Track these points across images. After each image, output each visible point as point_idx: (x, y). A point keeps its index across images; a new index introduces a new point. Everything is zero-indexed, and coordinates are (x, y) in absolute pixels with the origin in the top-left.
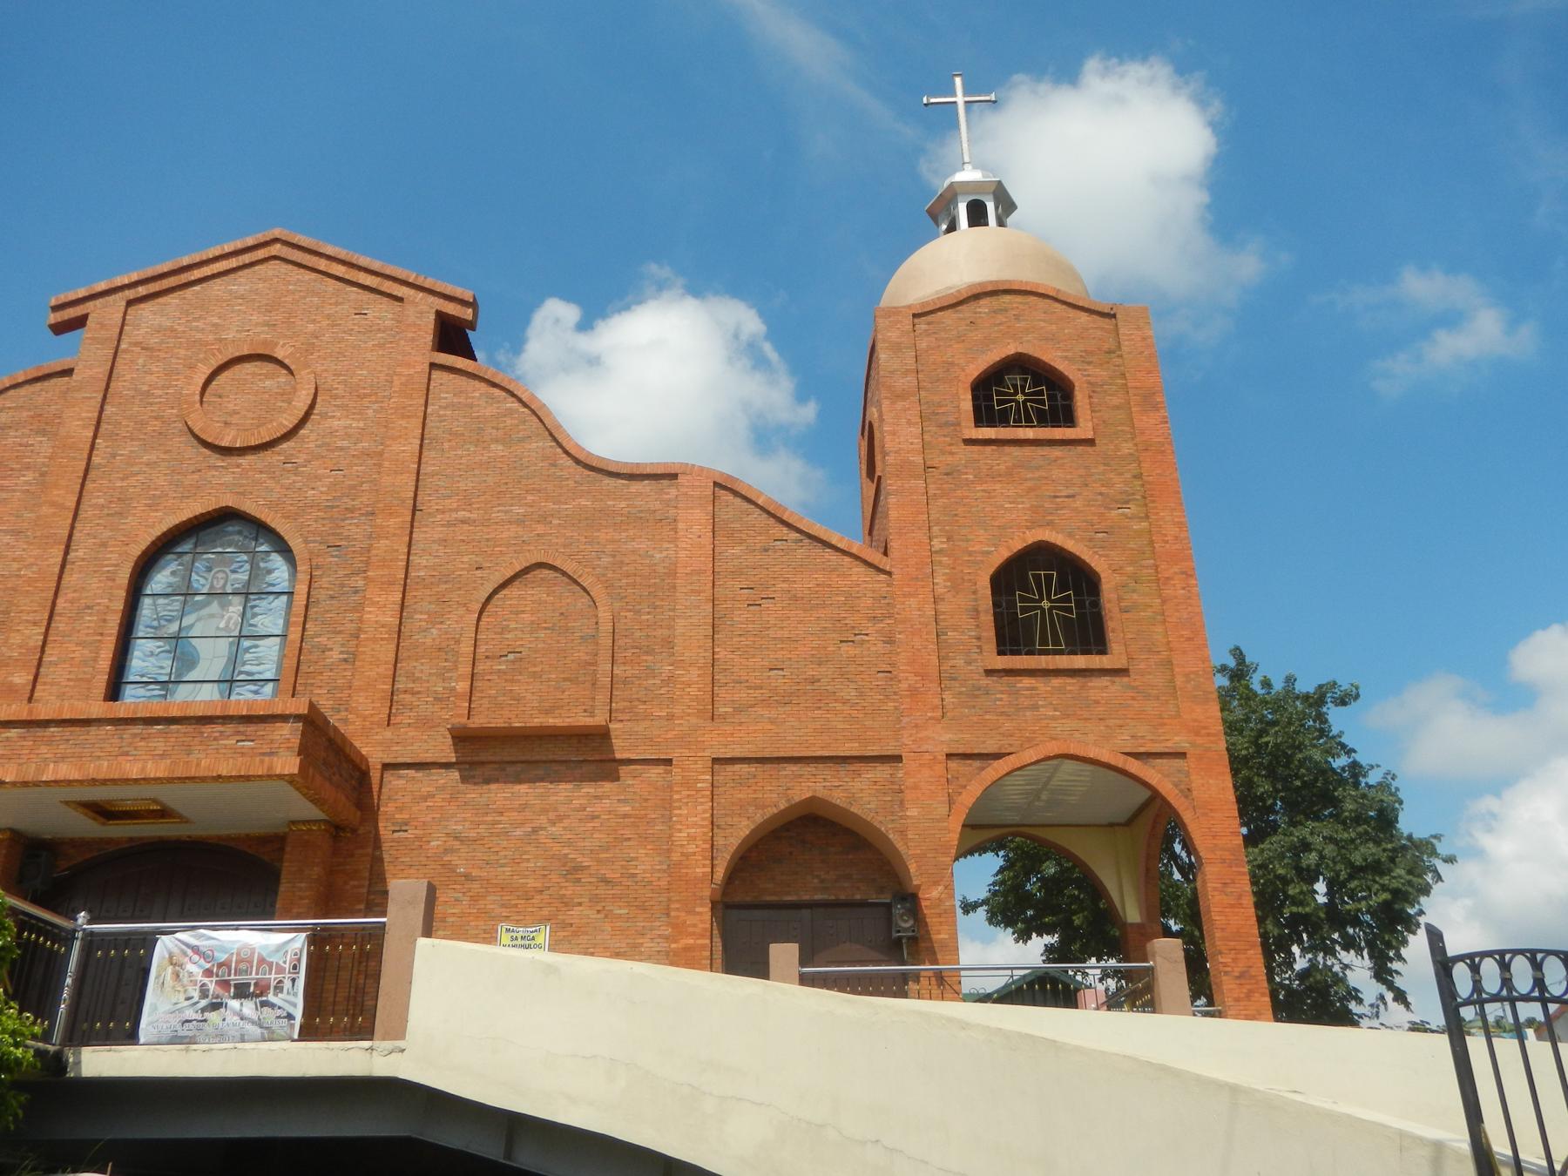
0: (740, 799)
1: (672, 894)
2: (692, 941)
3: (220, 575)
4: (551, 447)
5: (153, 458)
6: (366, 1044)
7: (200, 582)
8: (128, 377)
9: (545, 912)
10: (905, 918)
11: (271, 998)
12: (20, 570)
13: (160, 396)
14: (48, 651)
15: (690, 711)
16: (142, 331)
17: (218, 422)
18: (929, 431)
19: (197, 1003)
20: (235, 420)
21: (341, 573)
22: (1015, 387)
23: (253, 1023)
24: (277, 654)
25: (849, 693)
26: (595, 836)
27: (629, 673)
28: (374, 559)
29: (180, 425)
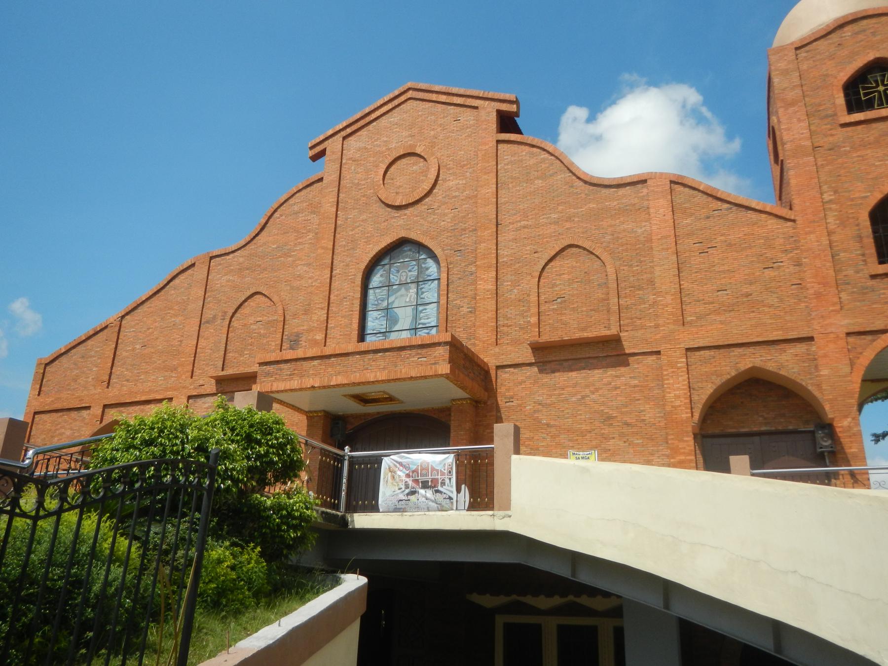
0: (706, 371)
1: (667, 431)
2: (683, 458)
3: (404, 274)
4: (569, 176)
5: (364, 217)
6: (491, 513)
7: (395, 279)
8: (348, 177)
9: (594, 443)
10: (825, 439)
11: (440, 488)
12: (312, 283)
13: (364, 185)
14: (330, 322)
15: (668, 321)
16: (352, 152)
17: (393, 193)
18: (814, 123)
19: (404, 491)
20: (401, 190)
21: (463, 264)
22: (876, 82)
23: (432, 501)
25: (773, 300)
26: (618, 399)
27: (629, 303)
28: (479, 255)
29: (375, 198)
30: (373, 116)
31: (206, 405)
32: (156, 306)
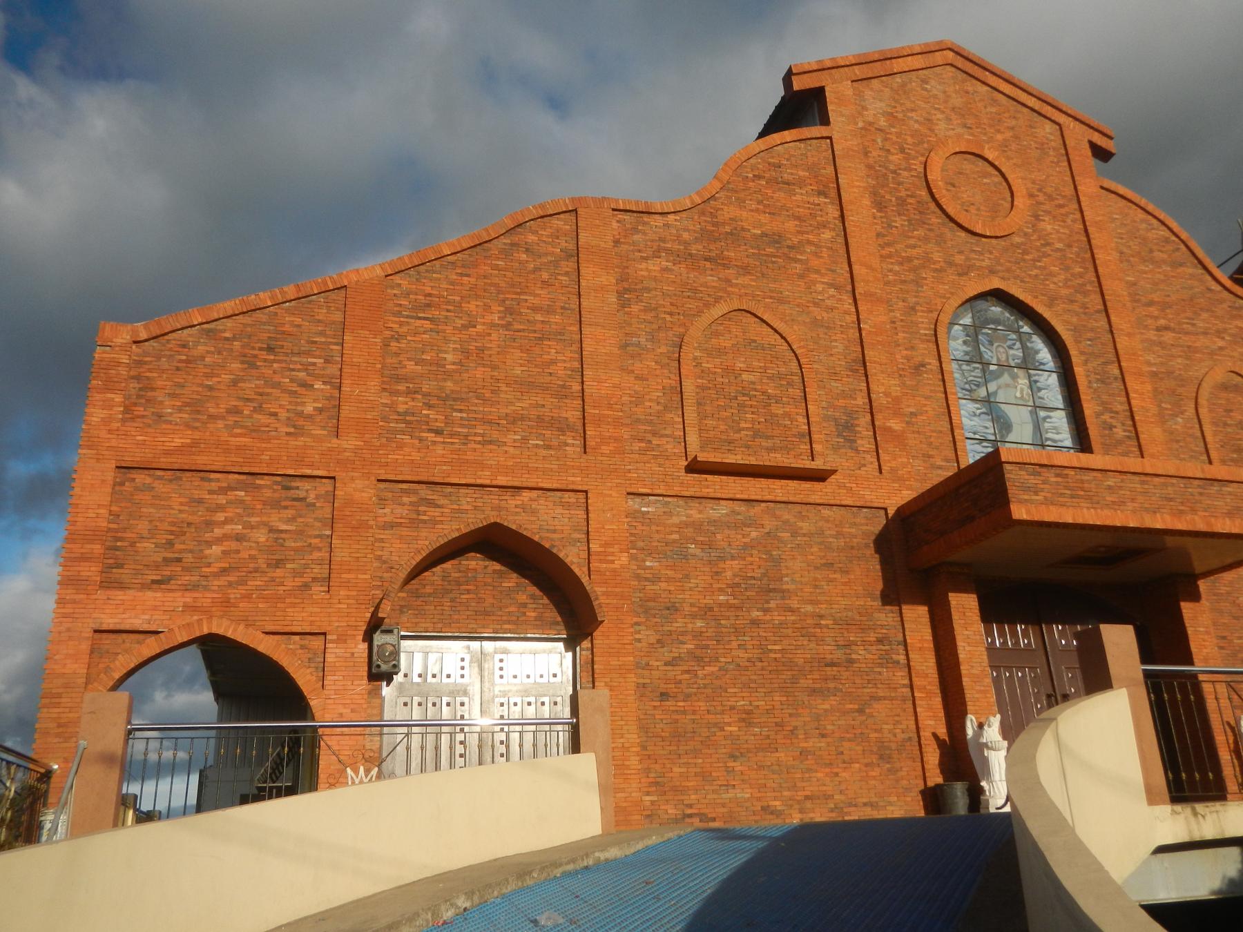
3: (1001, 350)
4: (1202, 274)
8: (875, 154)
24: (1066, 425)
30: (898, 65)
31: (675, 520)
32: (485, 277)
